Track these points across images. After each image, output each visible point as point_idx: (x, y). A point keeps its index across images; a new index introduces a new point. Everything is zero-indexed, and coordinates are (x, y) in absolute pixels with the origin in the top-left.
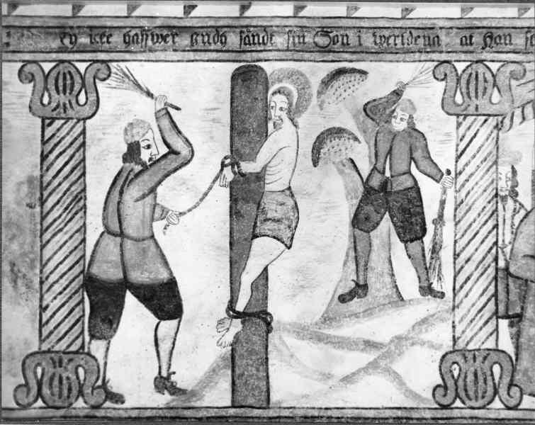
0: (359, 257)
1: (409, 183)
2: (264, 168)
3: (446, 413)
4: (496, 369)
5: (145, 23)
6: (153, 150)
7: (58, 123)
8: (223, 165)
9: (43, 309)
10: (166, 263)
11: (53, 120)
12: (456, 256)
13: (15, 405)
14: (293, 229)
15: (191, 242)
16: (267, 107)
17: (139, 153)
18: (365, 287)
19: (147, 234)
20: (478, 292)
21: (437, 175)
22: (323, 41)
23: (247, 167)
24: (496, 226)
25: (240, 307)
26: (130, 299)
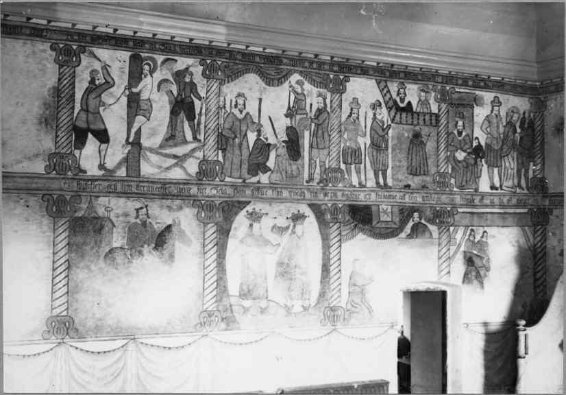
0: (173, 125)
1: (190, 100)
2: (140, 91)
3: (199, 182)
4: (217, 167)
5: (98, 34)
6: (100, 81)
7: (65, 67)
8: (126, 89)
9: (57, 137)
10: (104, 123)
11: (63, 66)
12: (205, 127)
13: (44, 172)
14: (150, 113)
15: (114, 118)
16: (142, 69)
17: (95, 81)
18: (175, 136)
19: (97, 111)
20: (212, 141)
21: (200, 98)
22: (163, 48)
23: (134, 90)
24: (219, 118)
25: (131, 140)
26: (90, 136)
